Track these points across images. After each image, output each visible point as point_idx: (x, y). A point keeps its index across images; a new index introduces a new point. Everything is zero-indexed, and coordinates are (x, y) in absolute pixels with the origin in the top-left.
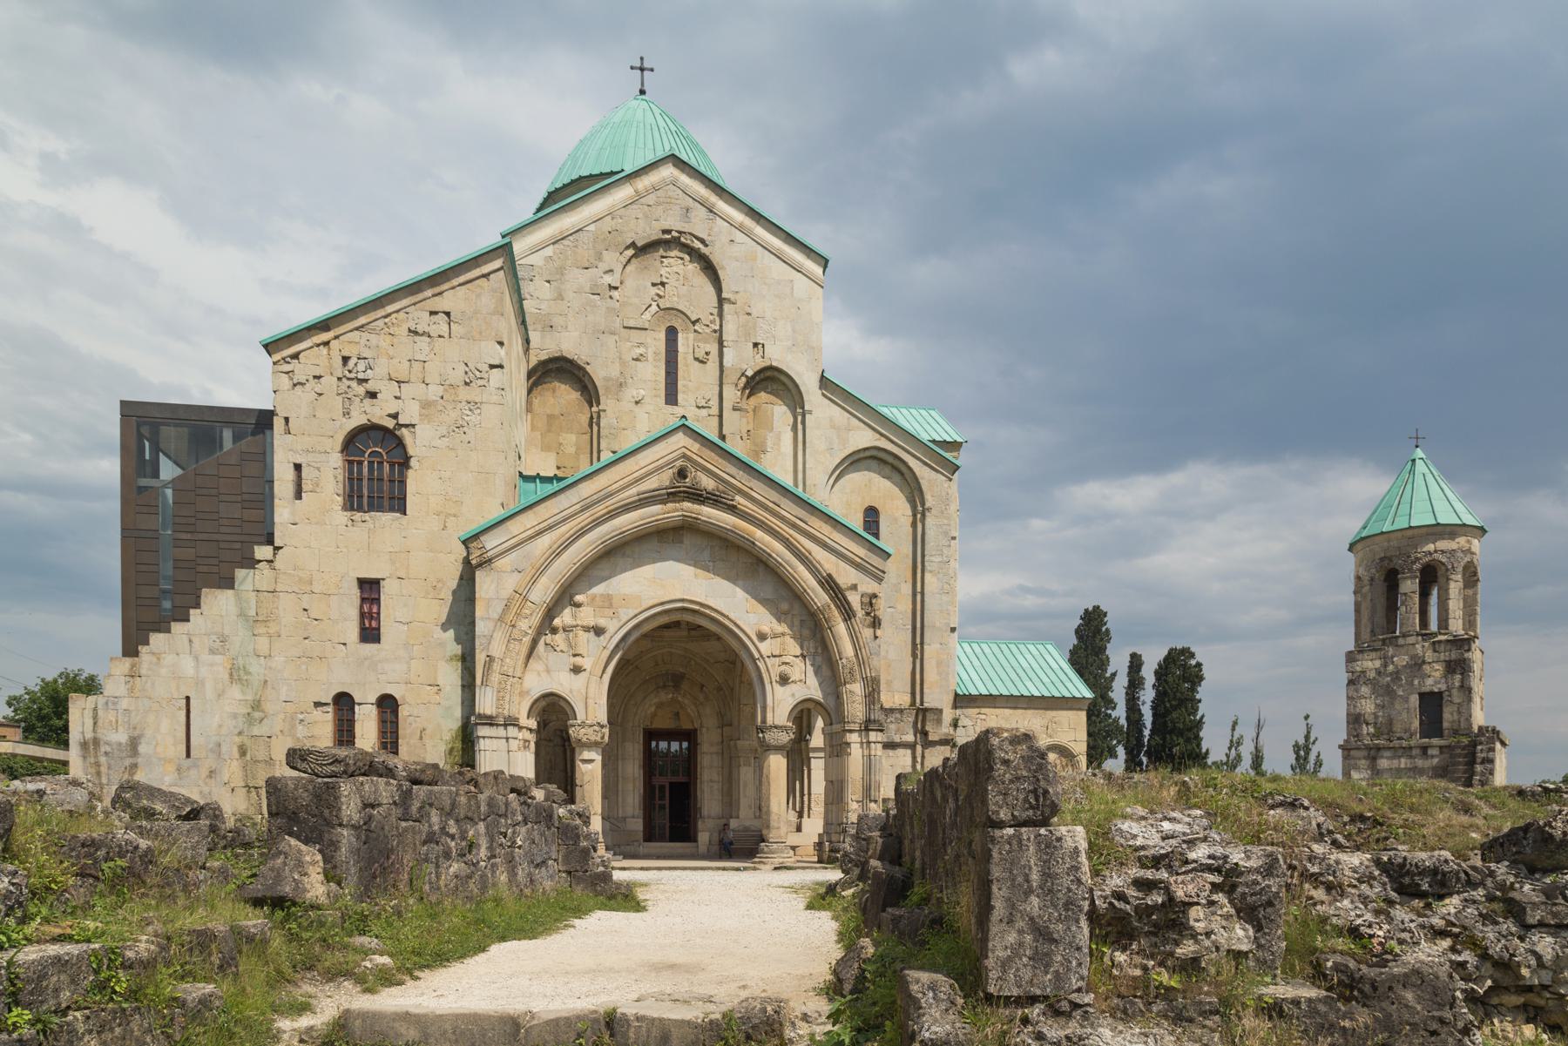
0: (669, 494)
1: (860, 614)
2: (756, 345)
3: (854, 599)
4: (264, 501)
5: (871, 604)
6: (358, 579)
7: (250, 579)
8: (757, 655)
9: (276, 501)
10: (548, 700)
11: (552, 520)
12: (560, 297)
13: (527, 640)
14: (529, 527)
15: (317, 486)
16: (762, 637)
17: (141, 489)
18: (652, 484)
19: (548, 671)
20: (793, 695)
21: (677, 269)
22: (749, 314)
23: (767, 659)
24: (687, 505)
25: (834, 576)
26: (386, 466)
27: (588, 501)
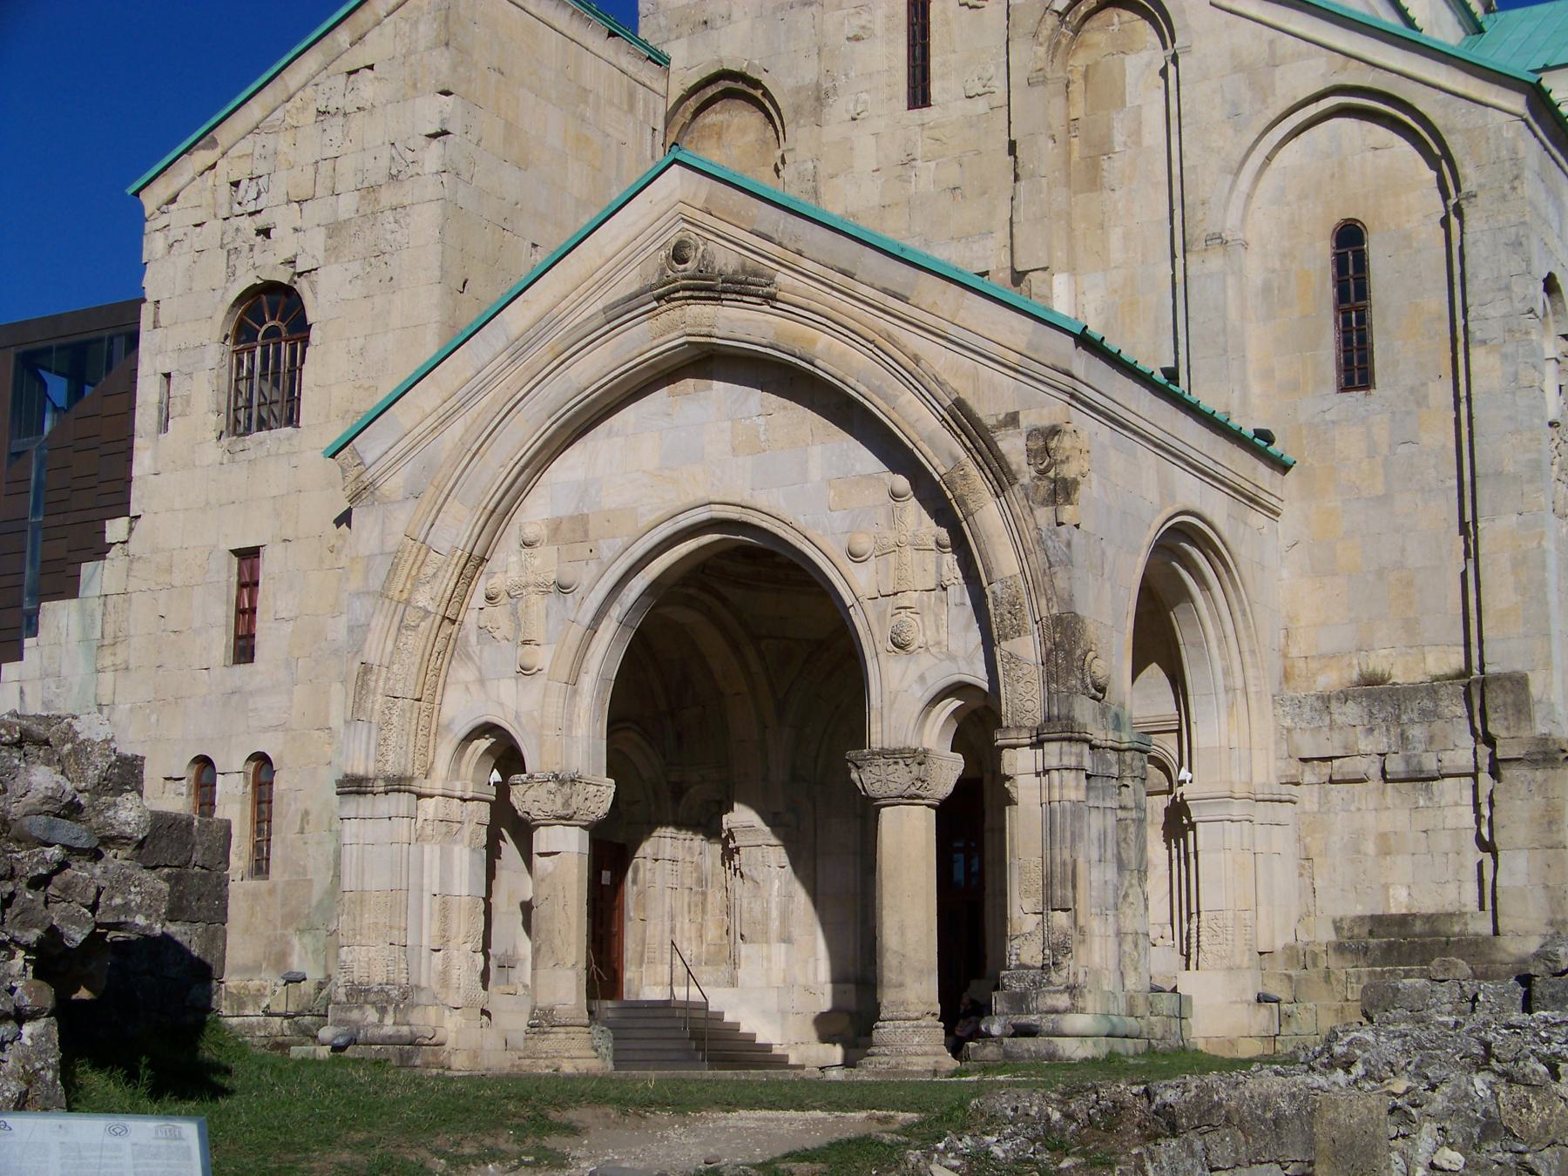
0: (658, 298)
1: (1026, 474)
3: (1013, 446)
5: (1047, 450)
6: (236, 552)
7: (97, 579)
8: (848, 600)
9: (138, 442)
11: (464, 390)
14: (428, 410)
15: (188, 402)
20: (922, 678)
23: (868, 604)
25: (971, 402)
27: (521, 342)
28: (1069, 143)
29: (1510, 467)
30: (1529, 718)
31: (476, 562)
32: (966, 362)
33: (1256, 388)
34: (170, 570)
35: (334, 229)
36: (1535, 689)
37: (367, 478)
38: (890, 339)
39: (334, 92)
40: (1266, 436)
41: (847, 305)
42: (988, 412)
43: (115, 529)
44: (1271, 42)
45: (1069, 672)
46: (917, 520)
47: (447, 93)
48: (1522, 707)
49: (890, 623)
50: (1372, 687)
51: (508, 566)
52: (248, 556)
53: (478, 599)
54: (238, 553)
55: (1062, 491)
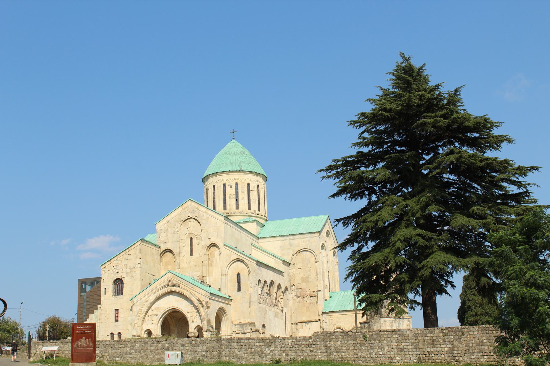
2: (209, 239)
3: (204, 303)
4: (100, 296)
8: (187, 317)
9: (101, 296)
10: (198, 327)
12: (167, 236)
13: (142, 319)
16: (188, 313)
17: (81, 296)
18: (164, 284)
19: (147, 325)
21: (192, 223)
22: (207, 232)
24: (171, 287)
26: (120, 286)
28: (209, 261)
29: (254, 301)
30: (255, 327)
31: (147, 312)
32: (199, 295)
33: (229, 291)
34: (107, 311)
35: (127, 273)
36: (256, 324)
37: (134, 303)
38: (192, 292)
39: (126, 257)
40: (229, 296)
41: (187, 288)
42: (201, 300)
43: (99, 306)
44: (231, 253)
45: (209, 325)
46: (194, 310)
47: (140, 259)
48: (255, 326)
49: (192, 319)
50: (240, 324)
51: (150, 312)
52: (117, 310)
53: (147, 316)
54: (116, 310)
55: (208, 308)
